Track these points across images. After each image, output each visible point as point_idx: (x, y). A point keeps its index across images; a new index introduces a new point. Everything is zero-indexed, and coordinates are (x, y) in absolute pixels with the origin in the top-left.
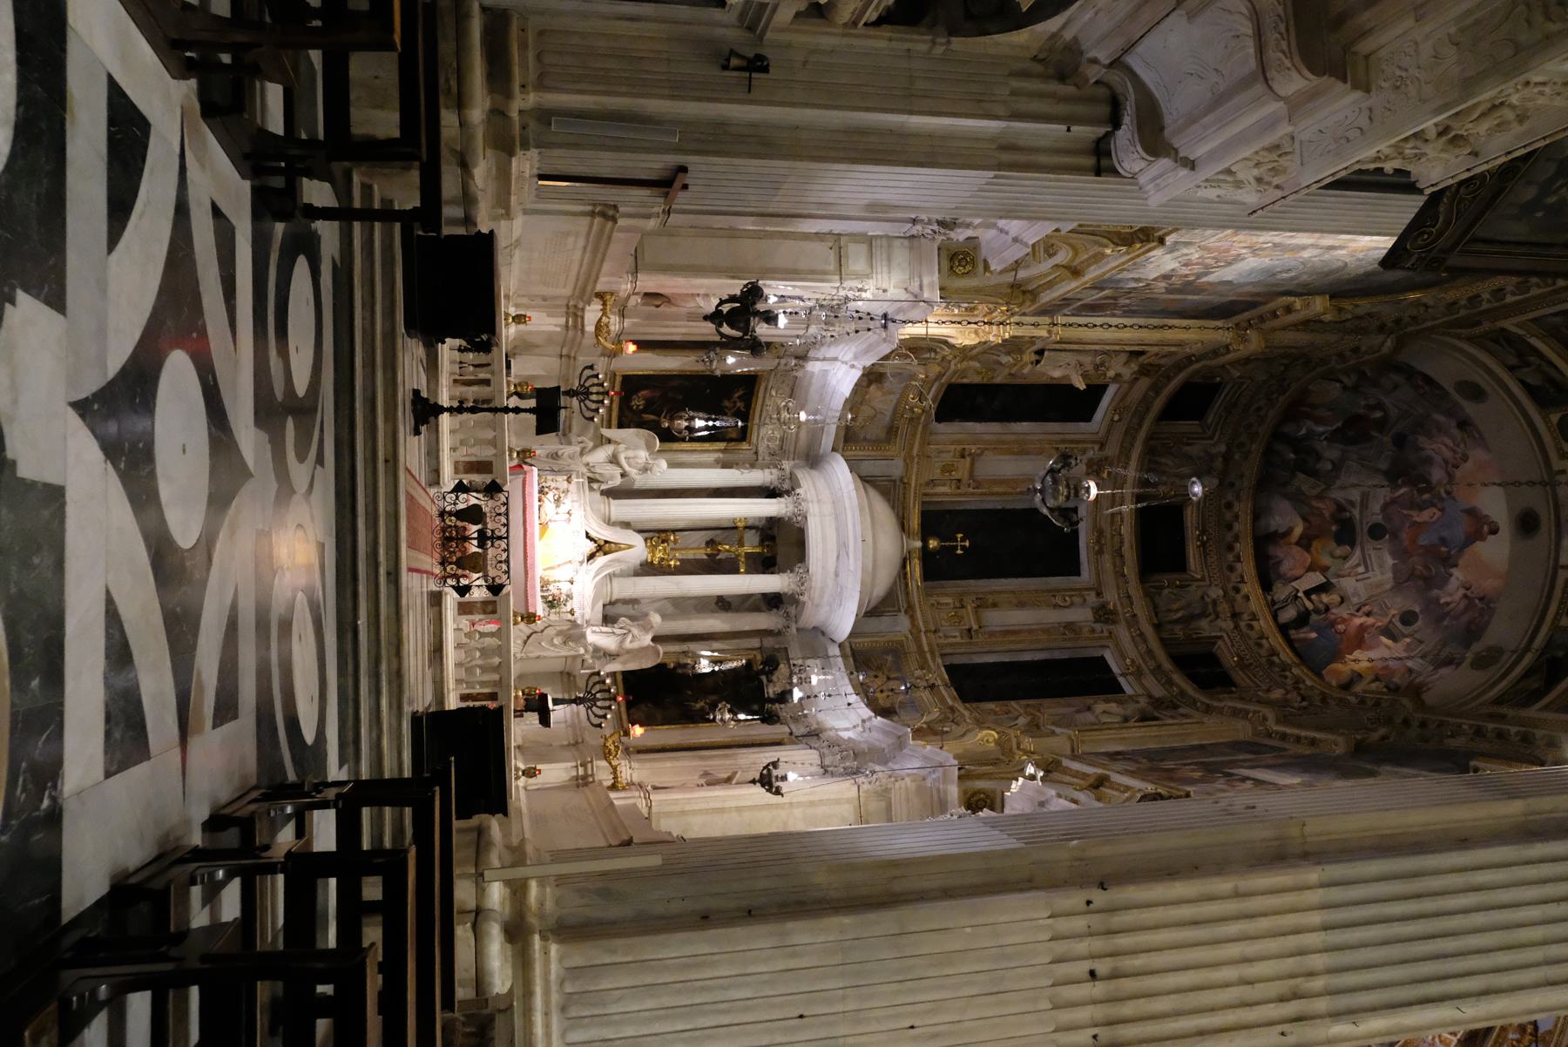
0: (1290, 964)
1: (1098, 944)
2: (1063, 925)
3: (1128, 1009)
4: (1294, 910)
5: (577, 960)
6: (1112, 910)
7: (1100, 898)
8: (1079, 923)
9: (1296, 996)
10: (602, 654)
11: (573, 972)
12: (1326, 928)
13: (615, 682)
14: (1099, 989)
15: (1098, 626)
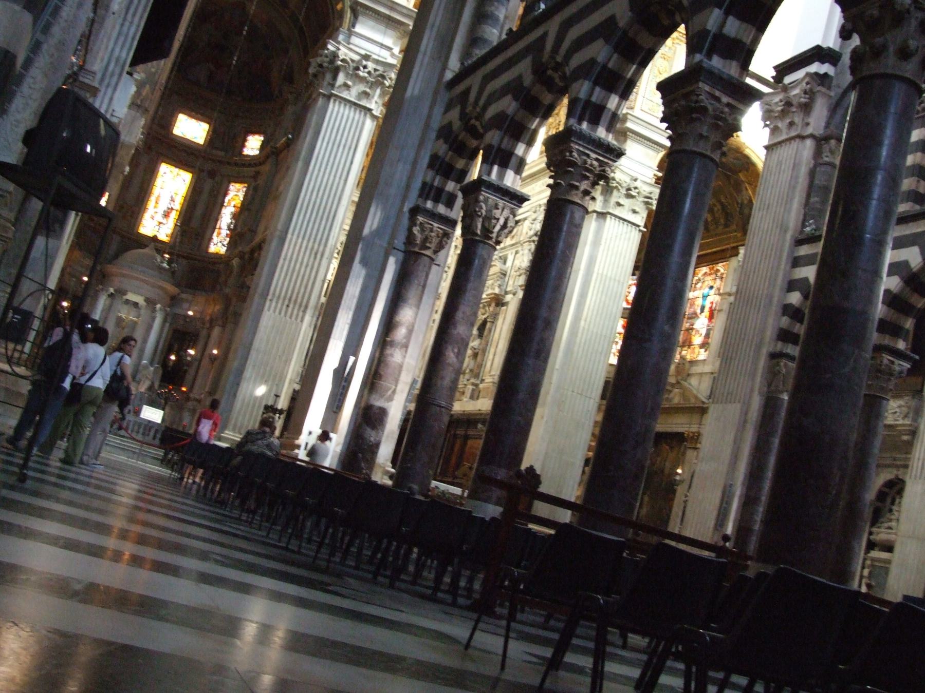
0: (308, 253)
1: (281, 301)
2: (272, 308)
3: (299, 300)
4: (295, 245)
5: (231, 427)
6: (274, 294)
7: (269, 297)
8: (274, 304)
9: (316, 254)
10: (151, 388)
11: (234, 430)
12: (303, 238)
13: (165, 387)
14: (291, 306)
15: (217, 179)
